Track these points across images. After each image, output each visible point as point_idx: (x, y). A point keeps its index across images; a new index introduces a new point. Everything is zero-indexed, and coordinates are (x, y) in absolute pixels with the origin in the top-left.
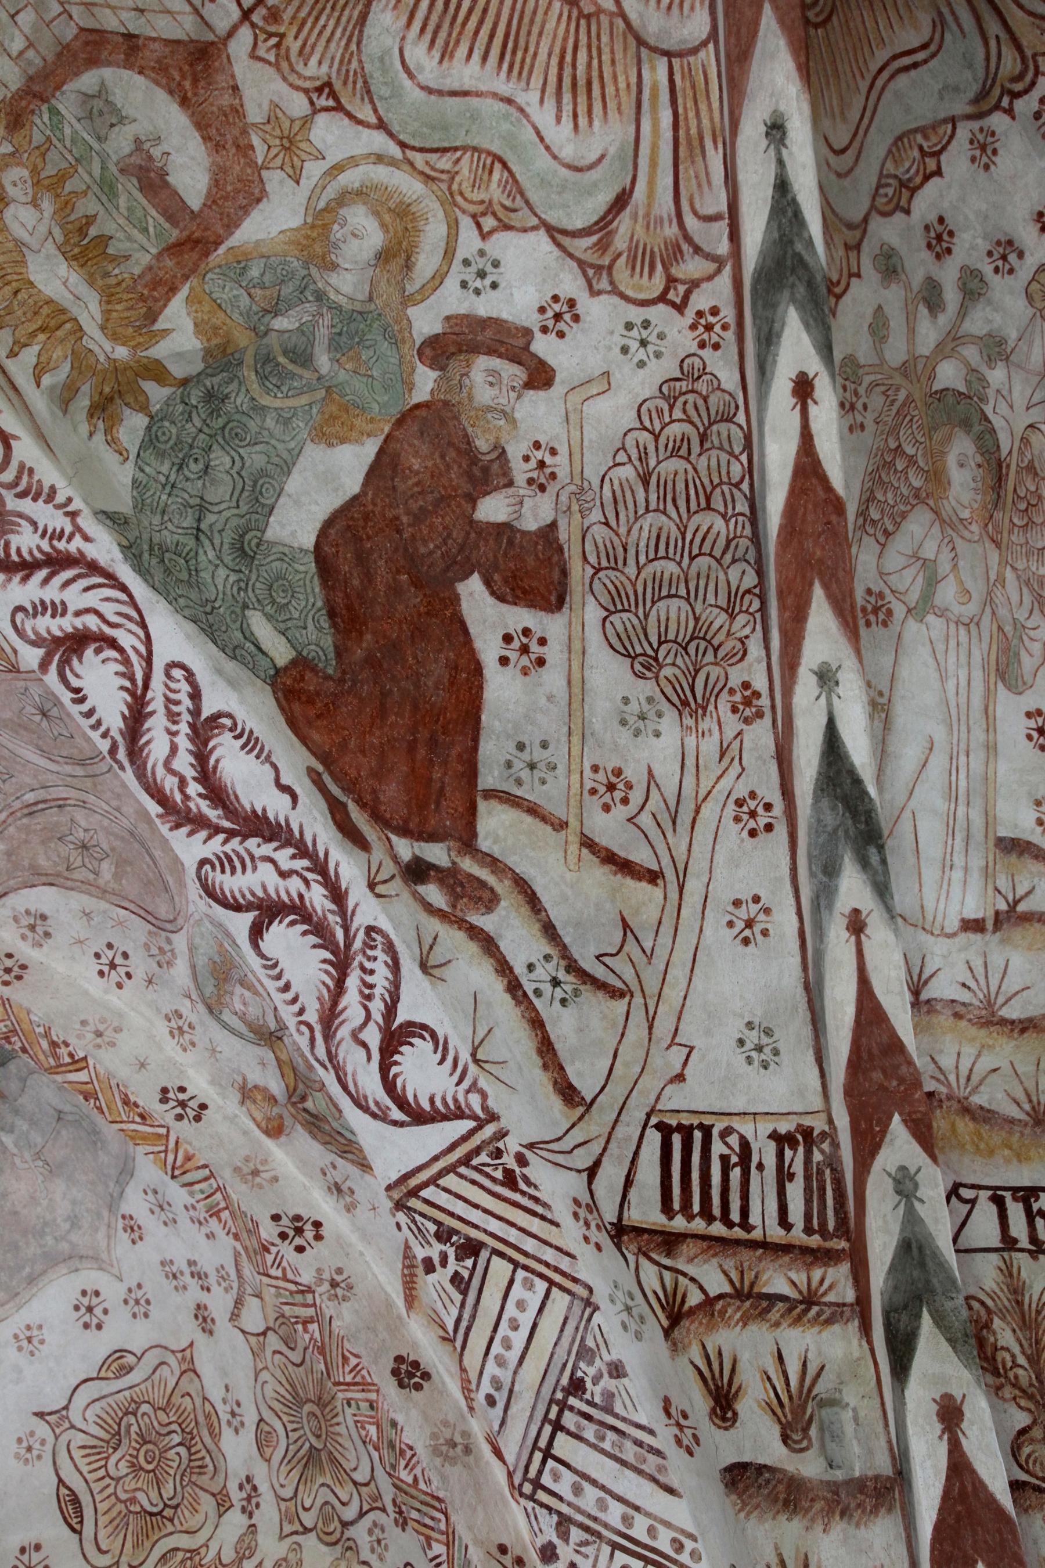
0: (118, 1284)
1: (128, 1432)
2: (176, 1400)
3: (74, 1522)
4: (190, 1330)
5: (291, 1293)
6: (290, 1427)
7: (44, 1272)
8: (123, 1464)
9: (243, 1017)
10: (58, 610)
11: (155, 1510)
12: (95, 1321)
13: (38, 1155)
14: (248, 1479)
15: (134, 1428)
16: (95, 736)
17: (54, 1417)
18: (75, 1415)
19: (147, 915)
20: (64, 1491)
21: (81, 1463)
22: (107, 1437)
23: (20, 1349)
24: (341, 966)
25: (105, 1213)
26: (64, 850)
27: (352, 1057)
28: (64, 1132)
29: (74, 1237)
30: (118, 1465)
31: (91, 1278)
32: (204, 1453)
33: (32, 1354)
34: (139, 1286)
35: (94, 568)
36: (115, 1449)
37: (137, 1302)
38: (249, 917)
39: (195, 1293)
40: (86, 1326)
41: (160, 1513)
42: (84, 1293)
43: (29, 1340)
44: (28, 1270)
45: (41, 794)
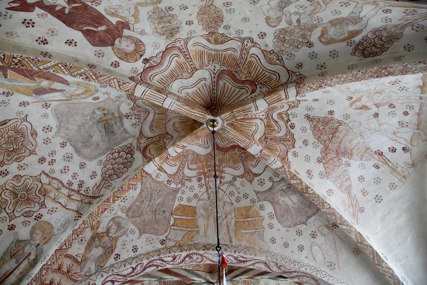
0: (52, 136)
2: (24, 148)
4: (40, 154)
5: (70, 241)
6: (21, 187)
7: (58, 120)
8: (11, 134)
9: (111, 227)
10: (179, 259)
12: (44, 129)
13: (83, 124)
14: (8, 172)
16: (164, 256)
18: (25, 123)
19: (130, 208)
21: (13, 125)
23: (44, 114)
24: (124, 276)
25: (67, 137)
26: (144, 197)
27: (112, 277)
28: (87, 135)
29: (64, 128)
30: (11, 133)
31: (54, 130)
32: (12, 156)
34: (50, 142)
35: (180, 263)
37: (47, 141)
38: (134, 267)
39: (48, 159)
40: (44, 127)
42: (51, 128)
43: (45, 116)
45: (153, 198)
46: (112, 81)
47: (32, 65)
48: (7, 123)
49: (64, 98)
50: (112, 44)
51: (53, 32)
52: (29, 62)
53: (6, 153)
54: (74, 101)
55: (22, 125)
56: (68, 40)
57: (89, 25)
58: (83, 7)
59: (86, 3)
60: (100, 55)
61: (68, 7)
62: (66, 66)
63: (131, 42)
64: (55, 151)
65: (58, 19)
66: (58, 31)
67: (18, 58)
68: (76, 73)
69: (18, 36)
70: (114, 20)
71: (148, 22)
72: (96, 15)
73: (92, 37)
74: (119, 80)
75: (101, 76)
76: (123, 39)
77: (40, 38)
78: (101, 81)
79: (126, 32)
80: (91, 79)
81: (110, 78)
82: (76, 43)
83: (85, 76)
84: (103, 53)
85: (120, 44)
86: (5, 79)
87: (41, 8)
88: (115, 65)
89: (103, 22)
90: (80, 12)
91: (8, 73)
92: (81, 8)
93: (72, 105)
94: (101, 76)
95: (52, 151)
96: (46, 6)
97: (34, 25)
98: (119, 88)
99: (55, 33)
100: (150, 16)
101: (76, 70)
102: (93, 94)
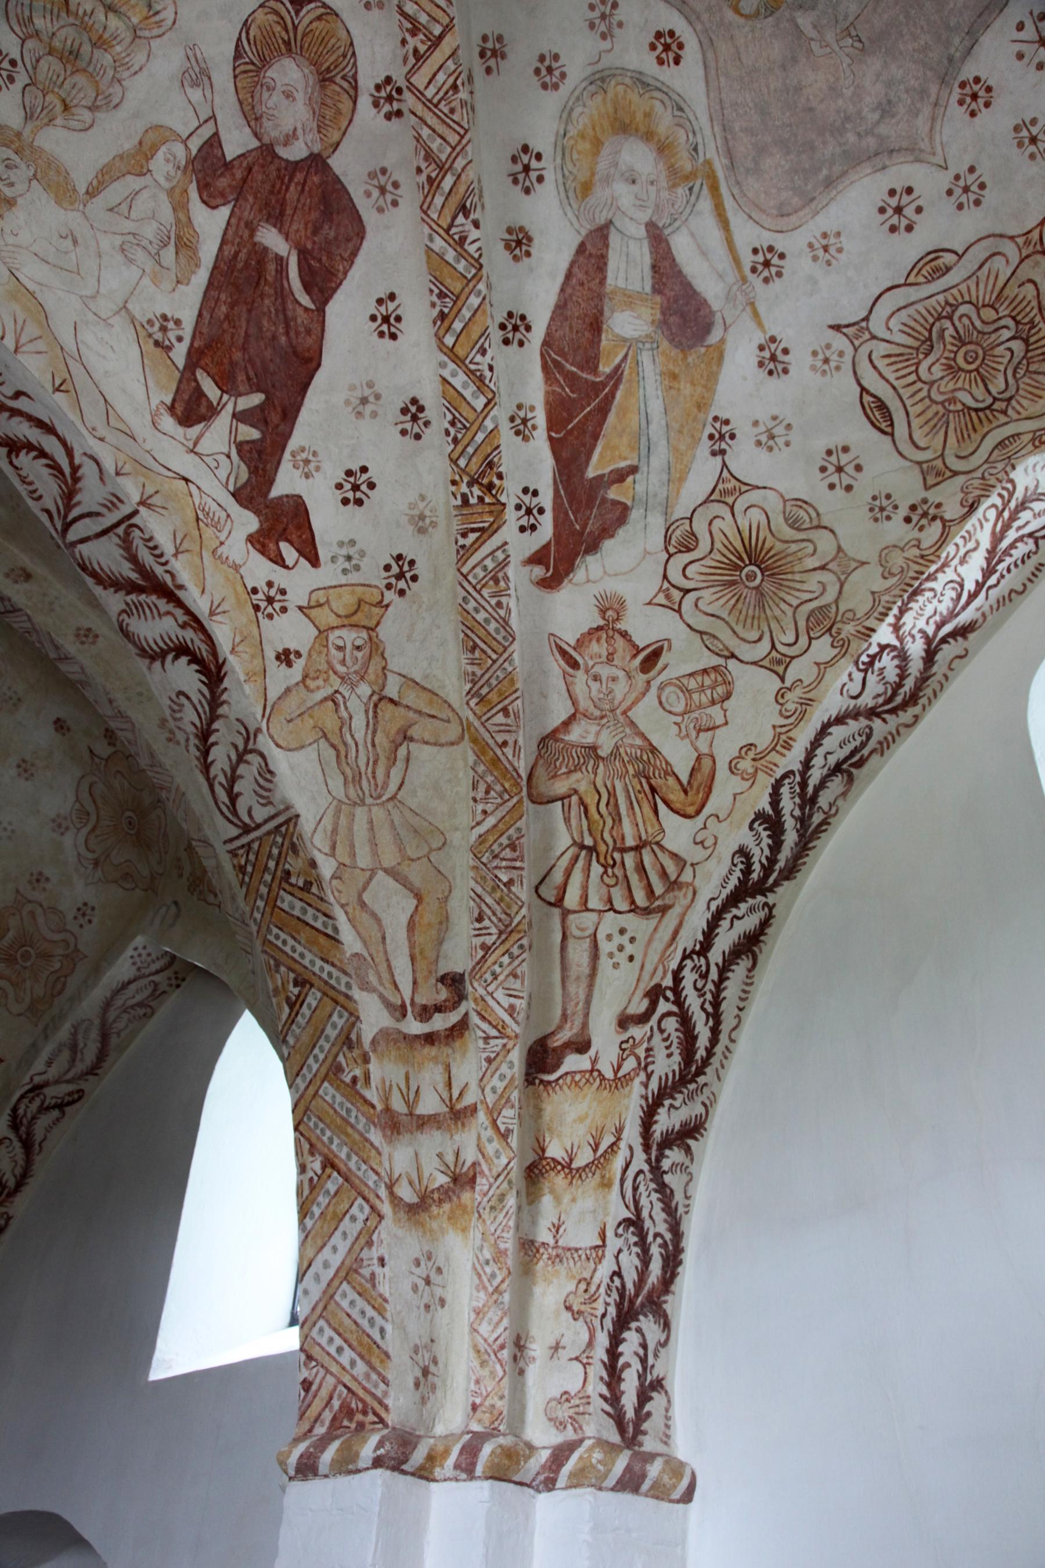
1: (941, 336)
2: (1011, 291)
3: (883, 426)
7: (844, 173)
11: (981, 405)
12: (904, 222)
15: (950, 331)
17: (855, 330)
18: (876, 325)
20: (867, 398)
21: (888, 372)
22: (916, 344)
23: (815, 258)
25: (934, 89)
29: (883, 130)
30: (932, 368)
31: (903, 172)
33: (829, 263)
34: (972, 170)
36: (927, 355)
37: (966, 190)
41: (989, 407)
42: (892, 193)
43: (826, 249)
44: (825, 172)
46: (429, 93)
47: (480, 437)
48: (878, 399)
49: (705, 204)
50: (317, 162)
51: (364, 401)
52: (470, 450)
53: (1032, 368)
54: (711, 151)
55: (887, 336)
56: (381, 334)
57: (283, 294)
58: (207, 360)
59: (180, 360)
60: (384, 184)
61: (230, 407)
62: (442, 316)
63: (266, 95)
64: (1017, 129)
65: (298, 410)
66: (352, 388)
67: (464, 488)
68: (461, 266)
69: (423, 498)
70: (211, 224)
71: (129, 95)
72: (223, 297)
73: (330, 255)
74: (412, 60)
75: (429, 156)
76: (274, 134)
77: (404, 432)
78: (453, 139)
79: (237, 142)
80: (462, 189)
81: (420, 109)
82: (380, 301)
83: (460, 220)
84: (372, 175)
85: (300, 132)
86: (644, 468)
87: (271, 482)
88: (390, 99)
89: (242, 256)
90: (237, 356)
91: (607, 471)
92: (220, 364)
93: (743, 147)
94: (429, 156)
95: (1020, 145)
96: (253, 471)
97: (355, 467)
98: (448, 38)
99: (367, 392)
100: (93, 108)
101: (446, 270)
102: (641, 82)
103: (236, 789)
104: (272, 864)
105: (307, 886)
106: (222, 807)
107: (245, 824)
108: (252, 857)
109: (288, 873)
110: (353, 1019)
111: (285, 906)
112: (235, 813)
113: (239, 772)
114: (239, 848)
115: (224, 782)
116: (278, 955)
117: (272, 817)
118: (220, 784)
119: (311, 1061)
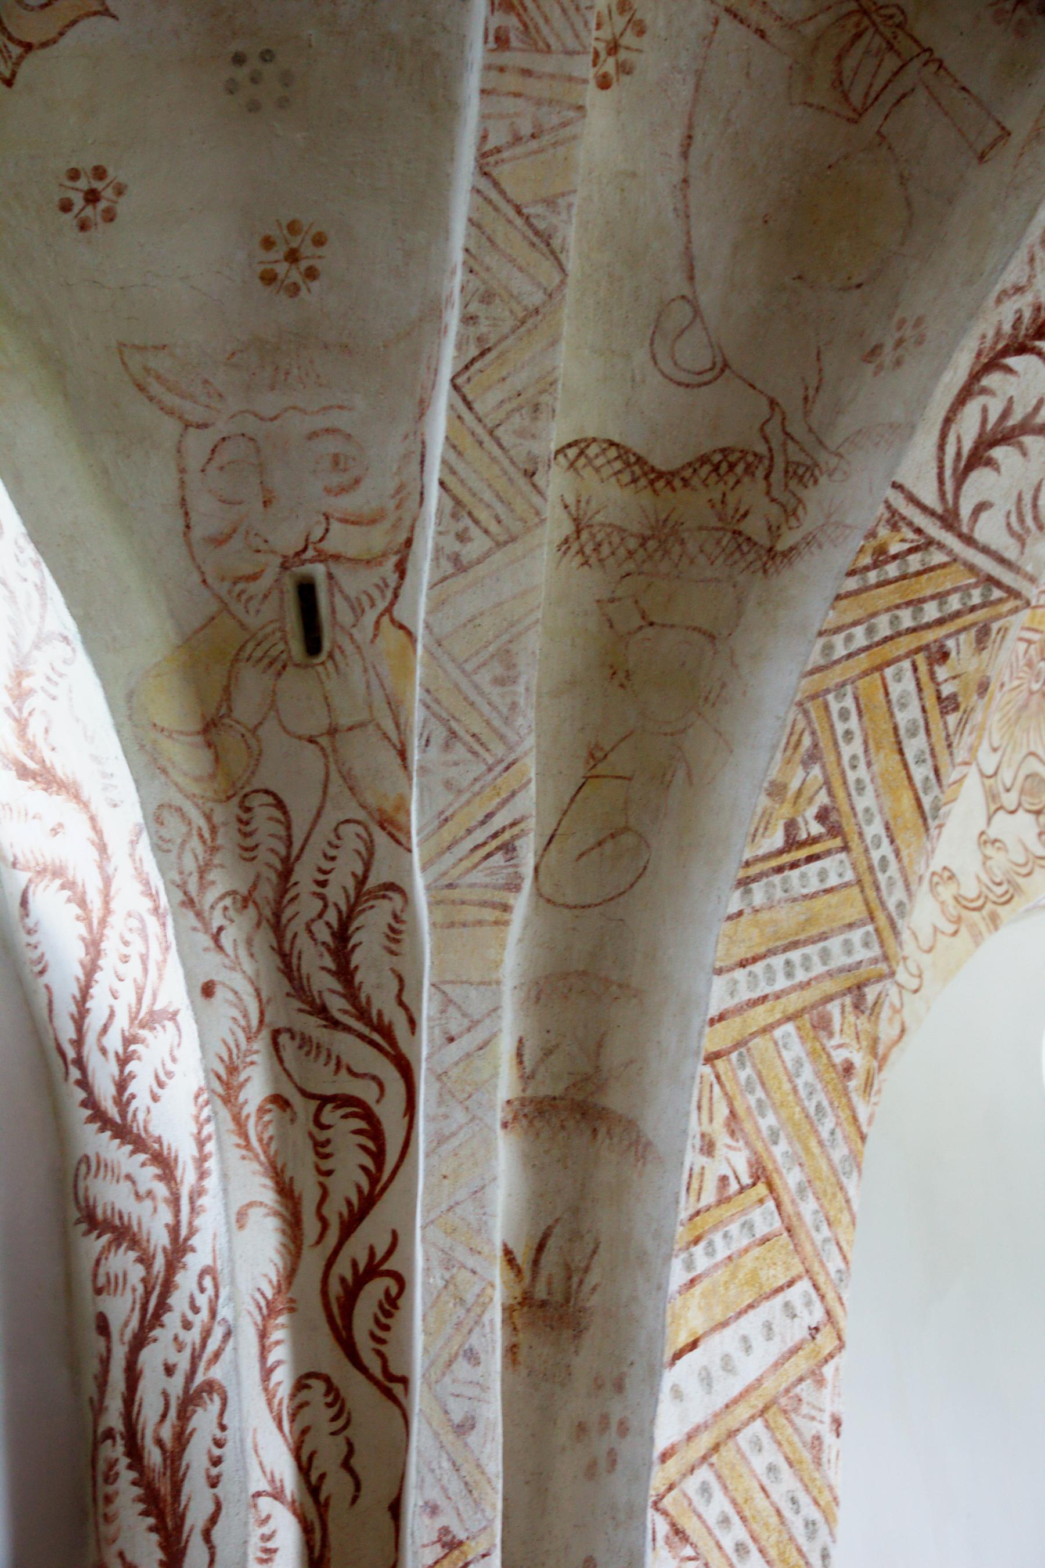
103: (998, 453)
104: (931, 611)
105: (948, 704)
106: (952, 439)
107: (956, 512)
108: (915, 562)
109: (945, 656)
110: (883, 967)
111: (895, 690)
112: (961, 477)
113: (1028, 440)
114: (910, 524)
115: (993, 417)
116: (824, 742)
117: (1002, 561)
118: (985, 410)
119: (777, 962)
